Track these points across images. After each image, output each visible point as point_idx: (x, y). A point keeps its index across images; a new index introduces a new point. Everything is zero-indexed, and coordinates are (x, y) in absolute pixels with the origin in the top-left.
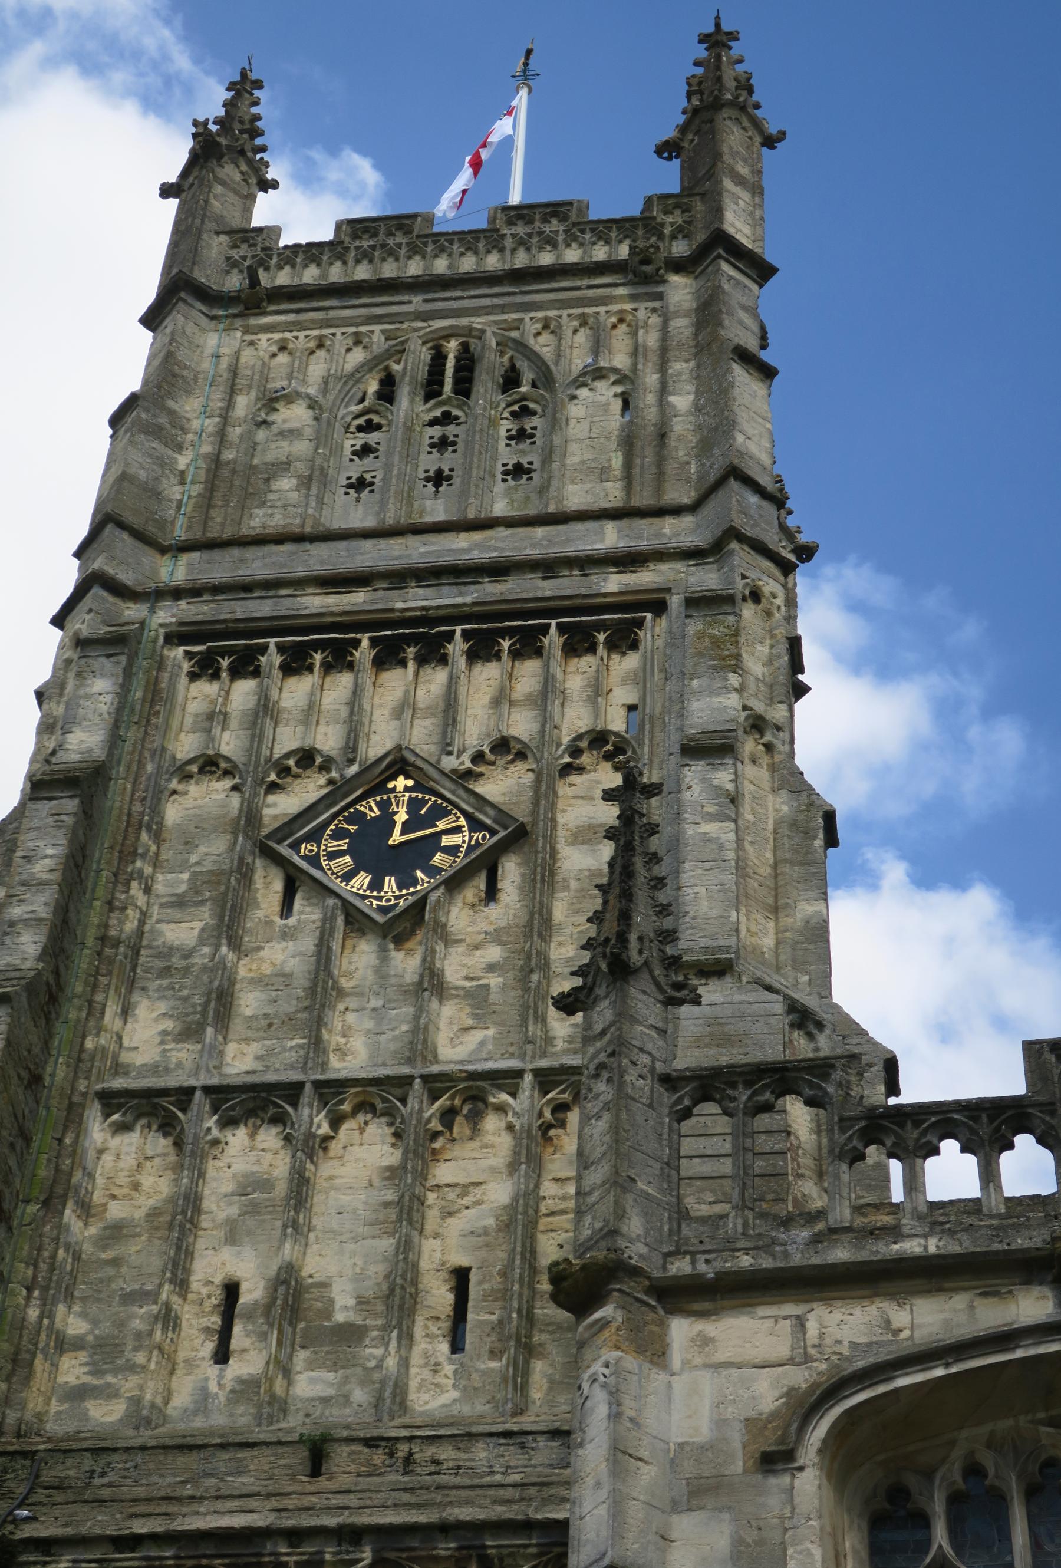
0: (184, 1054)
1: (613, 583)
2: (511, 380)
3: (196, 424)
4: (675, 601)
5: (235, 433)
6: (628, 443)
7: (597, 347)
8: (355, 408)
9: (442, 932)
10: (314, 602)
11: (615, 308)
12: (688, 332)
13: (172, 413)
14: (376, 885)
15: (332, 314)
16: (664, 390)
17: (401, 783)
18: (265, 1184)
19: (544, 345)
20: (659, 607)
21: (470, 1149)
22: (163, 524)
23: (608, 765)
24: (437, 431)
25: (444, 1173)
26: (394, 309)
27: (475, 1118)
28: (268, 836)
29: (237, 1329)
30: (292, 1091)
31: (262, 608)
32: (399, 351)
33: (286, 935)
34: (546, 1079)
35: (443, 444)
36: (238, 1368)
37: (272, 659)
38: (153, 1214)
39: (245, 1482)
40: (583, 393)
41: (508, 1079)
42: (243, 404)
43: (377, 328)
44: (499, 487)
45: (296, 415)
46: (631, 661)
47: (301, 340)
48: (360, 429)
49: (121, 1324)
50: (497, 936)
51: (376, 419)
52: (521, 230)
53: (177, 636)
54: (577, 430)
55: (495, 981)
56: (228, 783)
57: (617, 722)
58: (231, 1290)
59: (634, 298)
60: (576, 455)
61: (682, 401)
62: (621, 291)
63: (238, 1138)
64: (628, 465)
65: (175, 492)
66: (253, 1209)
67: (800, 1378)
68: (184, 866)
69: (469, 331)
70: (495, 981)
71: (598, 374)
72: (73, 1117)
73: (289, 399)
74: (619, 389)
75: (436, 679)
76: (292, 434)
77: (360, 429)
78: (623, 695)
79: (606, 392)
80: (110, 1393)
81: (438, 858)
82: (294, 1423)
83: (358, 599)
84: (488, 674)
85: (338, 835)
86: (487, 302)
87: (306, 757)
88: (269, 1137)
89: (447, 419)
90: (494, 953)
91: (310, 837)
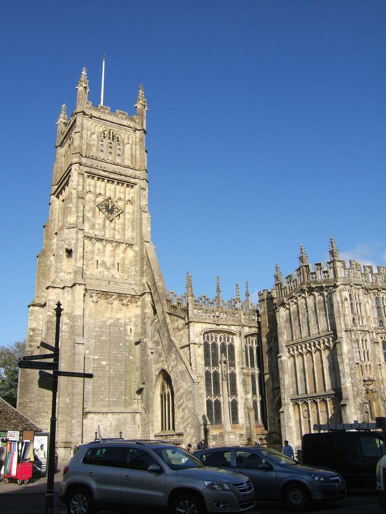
1: (132, 180)
4: (138, 185)
6: (132, 156)
7: (128, 139)
9: (115, 224)
10: (102, 173)
14: (108, 214)
16: (136, 150)
17: (110, 200)
18: (100, 250)
20: (136, 184)
21: (118, 249)
23: (130, 204)
24: (110, 145)
25: (116, 252)
27: (119, 246)
28: (98, 205)
29: (99, 266)
30: (103, 240)
32: (105, 131)
33: (100, 218)
38: (90, 251)
41: (123, 243)
44: (117, 157)
45: (94, 136)
46: (132, 190)
47: (95, 124)
49: (88, 263)
50: (120, 224)
53: (86, 172)
55: (120, 230)
56: (93, 195)
57: (131, 199)
58: (97, 261)
61: (138, 153)
64: (132, 160)
66: (99, 252)
67: (201, 329)
68: (88, 206)
70: (120, 230)
71: (128, 143)
80: (88, 271)
81: (114, 212)
85: (104, 206)
88: (100, 244)
89: (110, 143)
90: (120, 226)
91: (101, 206)
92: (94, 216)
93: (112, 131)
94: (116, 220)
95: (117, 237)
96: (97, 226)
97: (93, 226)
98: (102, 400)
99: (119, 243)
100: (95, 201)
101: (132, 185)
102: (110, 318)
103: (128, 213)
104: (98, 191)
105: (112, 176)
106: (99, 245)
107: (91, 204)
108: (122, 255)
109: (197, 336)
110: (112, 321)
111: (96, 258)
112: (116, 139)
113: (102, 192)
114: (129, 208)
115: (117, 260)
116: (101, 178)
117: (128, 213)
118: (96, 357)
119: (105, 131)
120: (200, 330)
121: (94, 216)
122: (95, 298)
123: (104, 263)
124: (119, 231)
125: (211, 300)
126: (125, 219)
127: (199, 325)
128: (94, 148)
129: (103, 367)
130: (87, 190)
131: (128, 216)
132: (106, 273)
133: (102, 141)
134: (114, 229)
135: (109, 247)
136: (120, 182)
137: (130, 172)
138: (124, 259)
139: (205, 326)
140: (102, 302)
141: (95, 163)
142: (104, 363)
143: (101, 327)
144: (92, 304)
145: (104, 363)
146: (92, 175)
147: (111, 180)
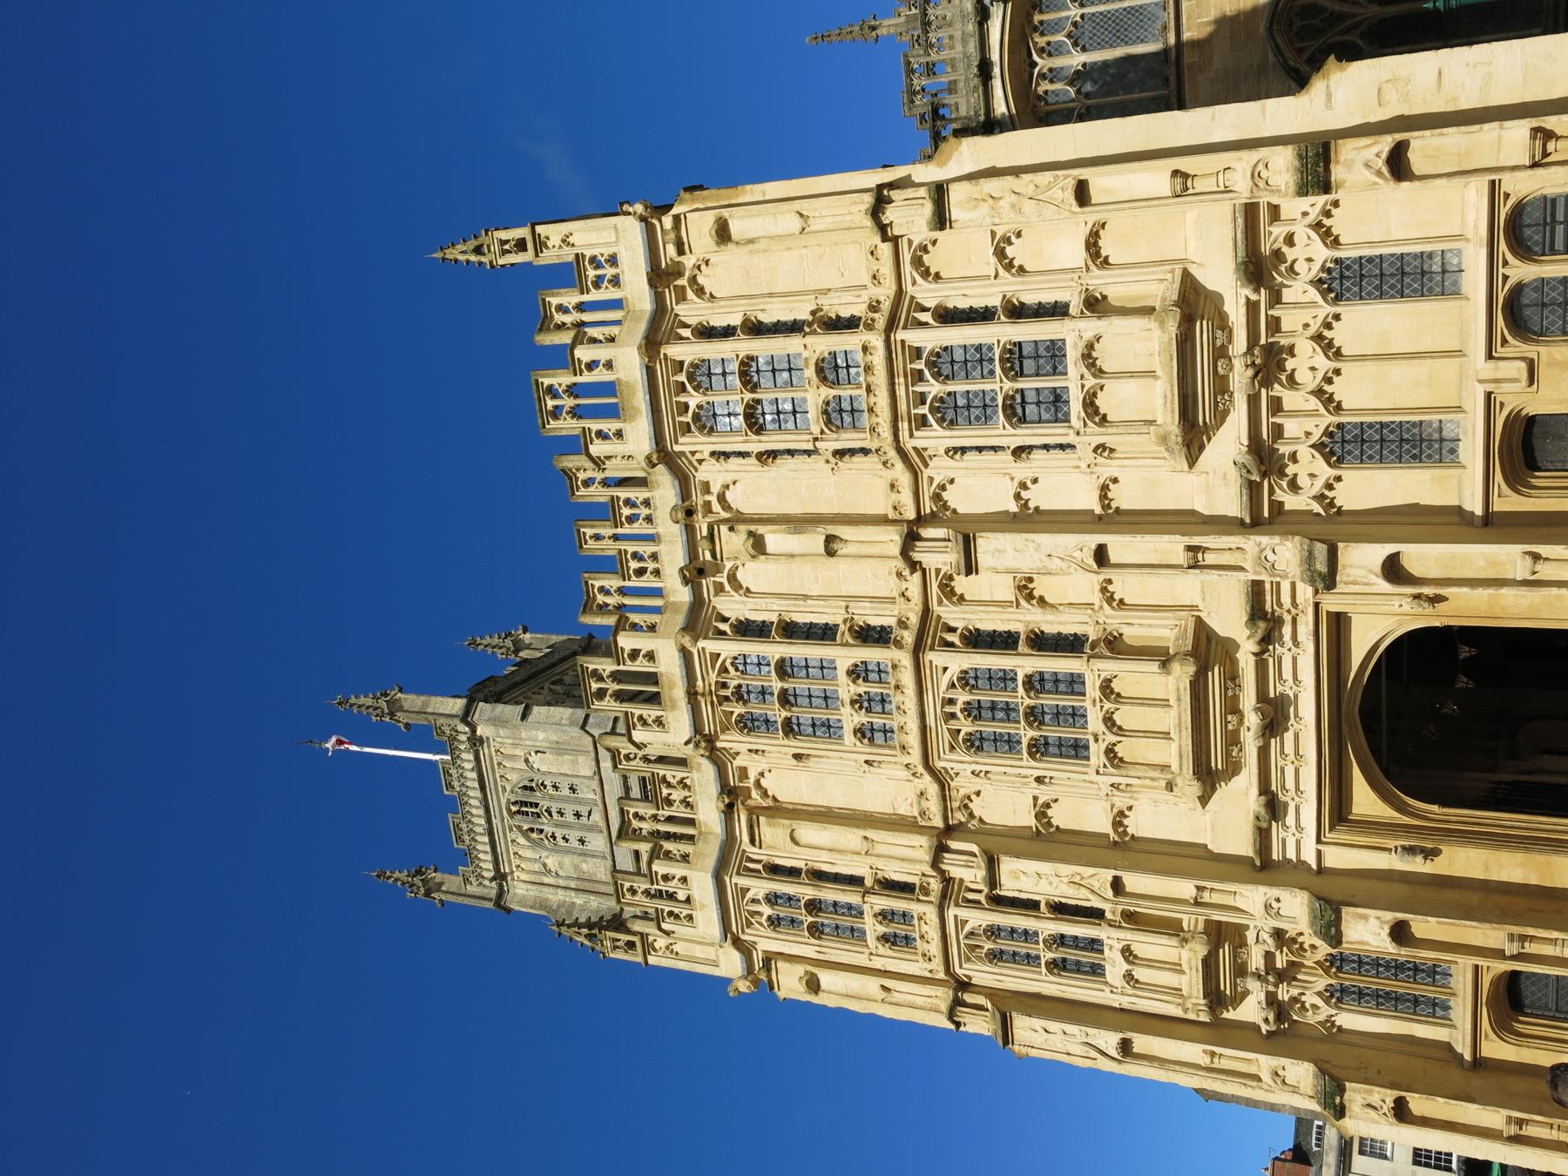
2: (532, 789)
3: (561, 898)
5: (561, 882)
8: (546, 842)
11: (494, 753)
12: (506, 730)
13: (559, 907)
15: (504, 850)
19: (513, 777)
24: (555, 816)
26: (500, 829)
32: (519, 828)
40: (535, 766)
42: (546, 880)
43: (508, 835)
45: (551, 862)
48: (555, 839)
51: (550, 834)
59: (489, 747)
61: (541, 736)
62: (486, 751)
69: (509, 802)
71: (527, 761)
73: (545, 865)
74: (533, 754)
76: (561, 865)
77: (555, 839)
79: (533, 758)
86: (495, 798)
93: (514, 809)
119: (519, 828)
128: (585, 867)
133: (554, 837)
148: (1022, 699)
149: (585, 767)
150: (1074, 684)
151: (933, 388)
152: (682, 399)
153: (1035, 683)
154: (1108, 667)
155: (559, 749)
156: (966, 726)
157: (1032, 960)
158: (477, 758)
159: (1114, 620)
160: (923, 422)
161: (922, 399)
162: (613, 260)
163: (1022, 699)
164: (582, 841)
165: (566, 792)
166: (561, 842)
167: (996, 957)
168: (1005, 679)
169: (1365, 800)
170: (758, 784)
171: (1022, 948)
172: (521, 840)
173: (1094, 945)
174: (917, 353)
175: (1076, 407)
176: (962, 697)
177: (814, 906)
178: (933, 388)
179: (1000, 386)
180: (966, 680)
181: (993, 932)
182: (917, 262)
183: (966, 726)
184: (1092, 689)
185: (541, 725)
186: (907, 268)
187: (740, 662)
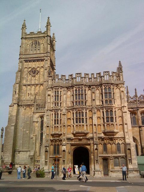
0: (26, 83)
1: (43, 58)
10: (30, 59)
22: (23, 53)
31: (28, 59)
32: (33, 41)
34: (40, 84)
35: (35, 47)
36: (29, 97)
37: (28, 62)
39: (30, 102)
41: (39, 84)
45: (28, 45)
46: (43, 62)
47: (28, 40)
52: (39, 33)
54: (41, 47)
60: (41, 49)
61: (46, 46)
63: (28, 87)
65: (23, 51)
72: (22, 86)
75: (35, 63)
78: (43, 64)
82: (31, 99)
83: (32, 59)
84: (38, 62)
87: (30, 67)
92: (27, 77)
94: (37, 76)
95: (37, 82)
96: (29, 80)
97: (27, 81)
98: (26, 146)
99: (37, 85)
100: (28, 71)
101: (42, 60)
102: (31, 114)
103: (42, 72)
104: (29, 66)
105: (34, 59)
106: (29, 87)
107: (27, 72)
108: (38, 89)
109: (36, 119)
110: (31, 115)
111: (28, 92)
112: (37, 44)
113: (31, 67)
114: (42, 70)
115: (36, 91)
116: (30, 61)
117: (42, 72)
118: (24, 130)
119: (33, 41)
120: (38, 116)
121: (27, 77)
122: (25, 108)
123: (31, 94)
124: (37, 80)
125: (132, 97)
126: (40, 74)
127: (38, 114)
128: (28, 50)
129: (27, 133)
130: (25, 67)
131: (41, 73)
132: (32, 97)
134: (35, 79)
135: (33, 87)
136: (38, 61)
137: (42, 55)
138: (39, 90)
139: (40, 114)
140: (28, 109)
141: (28, 56)
142: (27, 132)
143: (27, 118)
144: (24, 110)
145: (27, 132)
146: (26, 61)
147: (34, 61)
148: (81, 117)
149: (42, 52)
150: (83, 122)
151: (109, 110)
152: (107, 86)
153: (83, 119)
154: (85, 125)
155: (44, 48)
156: (78, 112)
157: (55, 118)
158: (42, 37)
159: (88, 125)
160: (106, 109)
161: (108, 109)
162: (119, 80)
163: (81, 117)
164: (32, 50)
165: (38, 48)
166: (31, 47)
167: (55, 114)
168: (83, 116)
169: (73, 147)
170: (69, 90)
171: (56, 117)
172: (31, 42)
173: (58, 123)
174: (112, 109)
175: (108, 123)
176: (81, 112)
177: (58, 96)
178: (109, 110)
179: (110, 116)
180: (83, 113)
181: (58, 114)
182: (119, 109)
183: (78, 112)
184: (83, 124)
185: (47, 46)
186: (119, 108)
187: (82, 90)
